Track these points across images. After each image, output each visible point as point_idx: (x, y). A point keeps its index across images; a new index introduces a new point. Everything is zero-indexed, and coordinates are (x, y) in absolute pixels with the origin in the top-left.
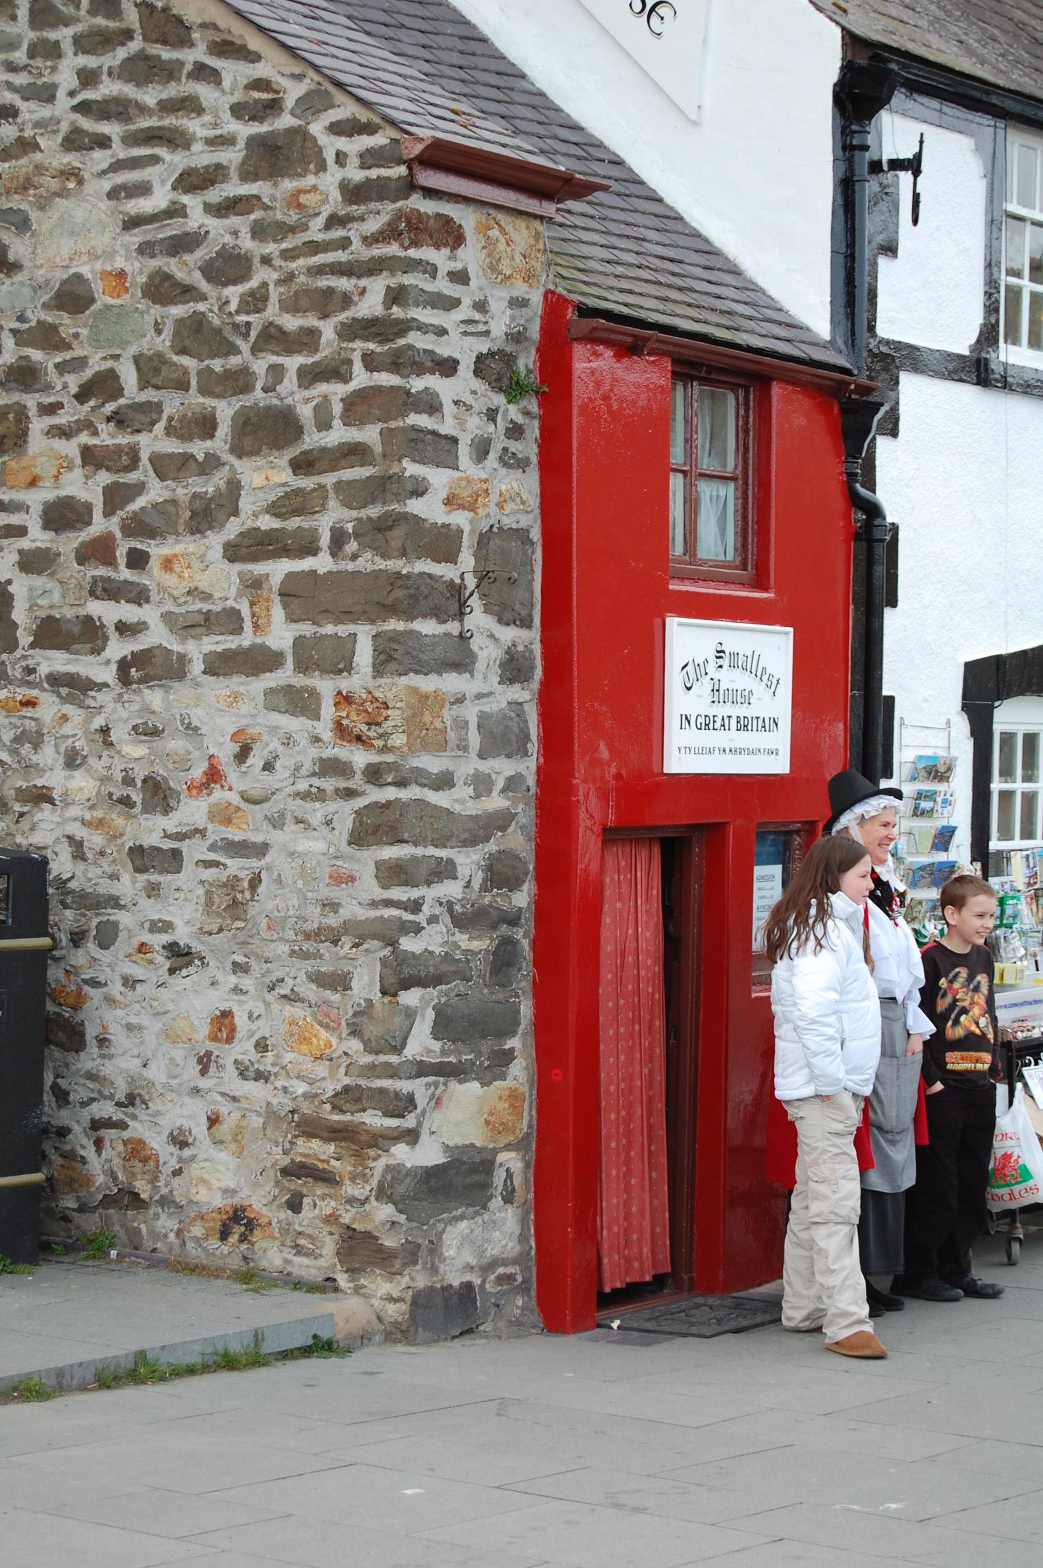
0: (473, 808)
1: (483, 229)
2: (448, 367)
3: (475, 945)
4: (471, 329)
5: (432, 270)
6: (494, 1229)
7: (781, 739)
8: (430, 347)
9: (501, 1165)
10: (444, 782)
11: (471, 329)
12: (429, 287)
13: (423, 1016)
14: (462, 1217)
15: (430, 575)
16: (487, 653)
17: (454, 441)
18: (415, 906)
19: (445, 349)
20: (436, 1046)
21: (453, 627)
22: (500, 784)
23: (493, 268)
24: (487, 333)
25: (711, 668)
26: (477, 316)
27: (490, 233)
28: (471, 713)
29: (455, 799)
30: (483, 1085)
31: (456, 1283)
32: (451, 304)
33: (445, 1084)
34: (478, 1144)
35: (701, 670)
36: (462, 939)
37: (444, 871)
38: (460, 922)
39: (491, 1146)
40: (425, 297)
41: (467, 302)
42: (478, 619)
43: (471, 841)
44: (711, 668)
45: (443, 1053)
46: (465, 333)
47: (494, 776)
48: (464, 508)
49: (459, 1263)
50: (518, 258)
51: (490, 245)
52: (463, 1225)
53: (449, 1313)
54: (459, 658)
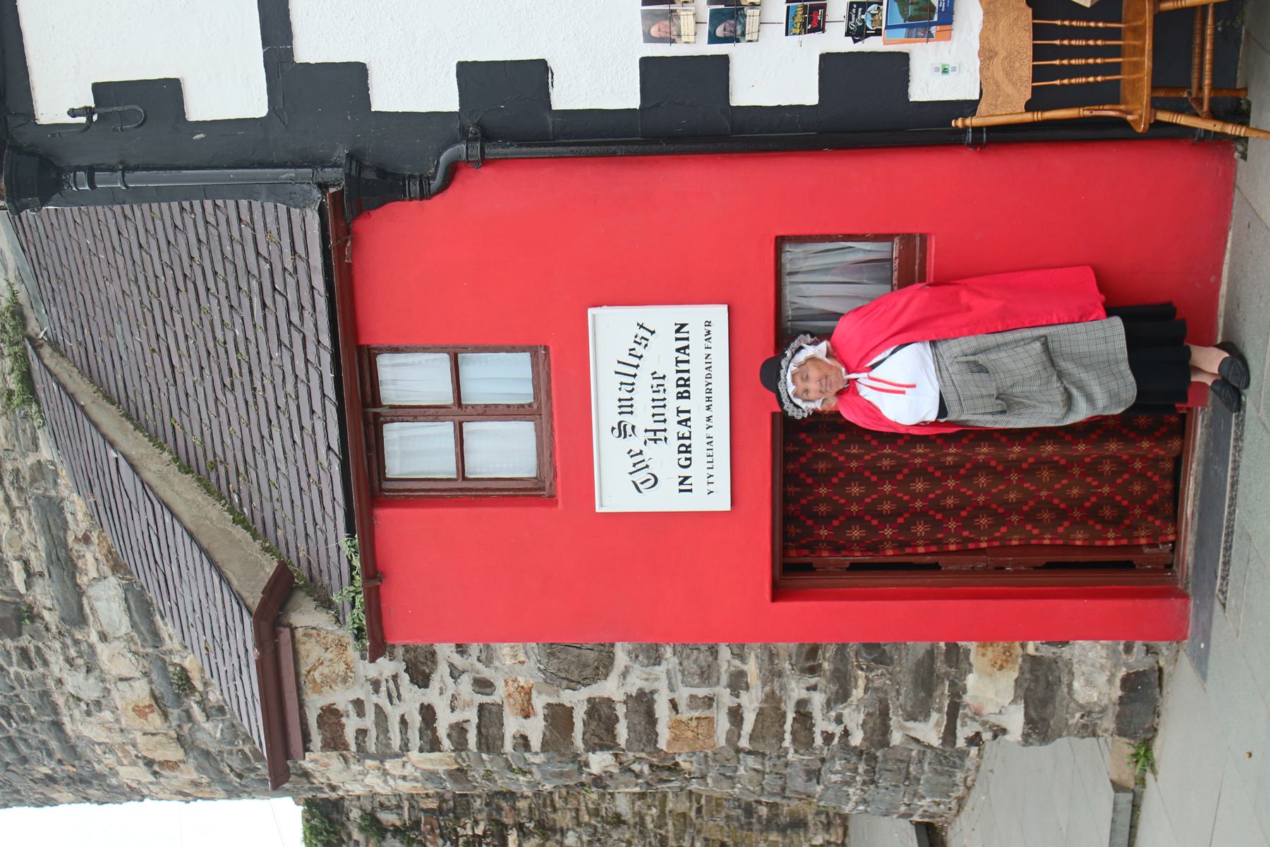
1: (317, 689)
2: (428, 713)
3: (861, 683)
4: (395, 694)
5: (362, 733)
6: (1086, 656)
8: (417, 733)
9: (1037, 649)
11: (395, 694)
12: (373, 733)
13: (910, 729)
14: (1070, 686)
15: (584, 734)
16: (635, 683)
17: (481, 707)
18: (828, 737)
19: (416, 720)
20: (935, 716)
21: (621, 710)
22: (737, 662)
23: (345, 680)
24: (395, 677)
26: (383, 689)
27: (319, 681)
30: (970, 671)
31: (1120, 693)
33: (965, 706)
34: (1015, 675)
35: (639, 462)
36: (858, 693)
38: (842, 695)
39: (1020, 660)
40: (381, 737)
41: (375, 699)
42: (610, 688)
44: (635, 443)
45: (939, 710)
46: (399, 697)
47: (732, 669)
48: (530, 699)
49: (1105, 689)
50: (329, 655)
51: (329, 682)
52: (1076, 685)
53: (1141, 696)
54: (643, 703)
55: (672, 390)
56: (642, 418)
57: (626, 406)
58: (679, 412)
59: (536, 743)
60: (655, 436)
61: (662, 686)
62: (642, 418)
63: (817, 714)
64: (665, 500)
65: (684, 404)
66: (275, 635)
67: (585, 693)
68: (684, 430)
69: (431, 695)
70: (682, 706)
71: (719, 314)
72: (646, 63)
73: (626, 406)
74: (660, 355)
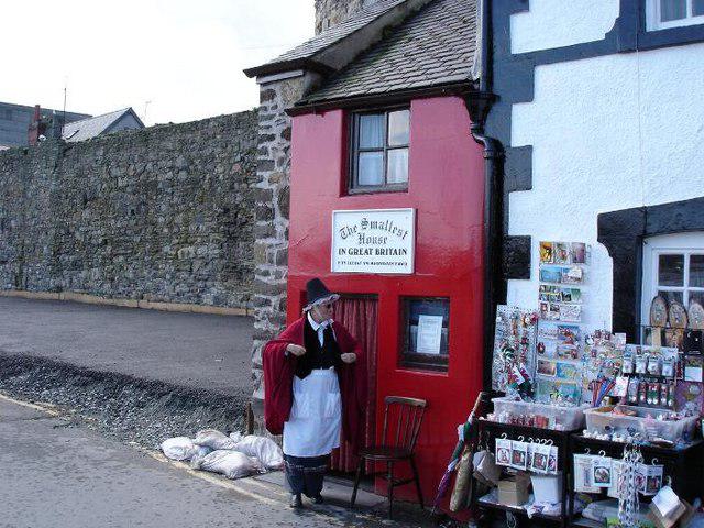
0: (276, 282)
2: (272, 138)
7: (409, 258)
10: (266, 274)
25: (359, 230)
28: (275, 252)
29: (270, 280)
32: (271, 117)
37: (267, 303)
43: (274, 294)
55: (380, 247)
56: (369, 233)
57: (374, 225)
58: (371, 249)
59: (259, 185)
60: (361, 238)
61: (278, 242)
62: (369, 233)
63: (264, 309)
64: (338, 243)
65: (374, 252)
66: (300, 68)
67: (276, 206)
68: (366, 252)
69: (278, 138)
70: (270, 250)
71: (408, 270)
72: (528, 239)
73: (374, 225)
74: (394, 242)
